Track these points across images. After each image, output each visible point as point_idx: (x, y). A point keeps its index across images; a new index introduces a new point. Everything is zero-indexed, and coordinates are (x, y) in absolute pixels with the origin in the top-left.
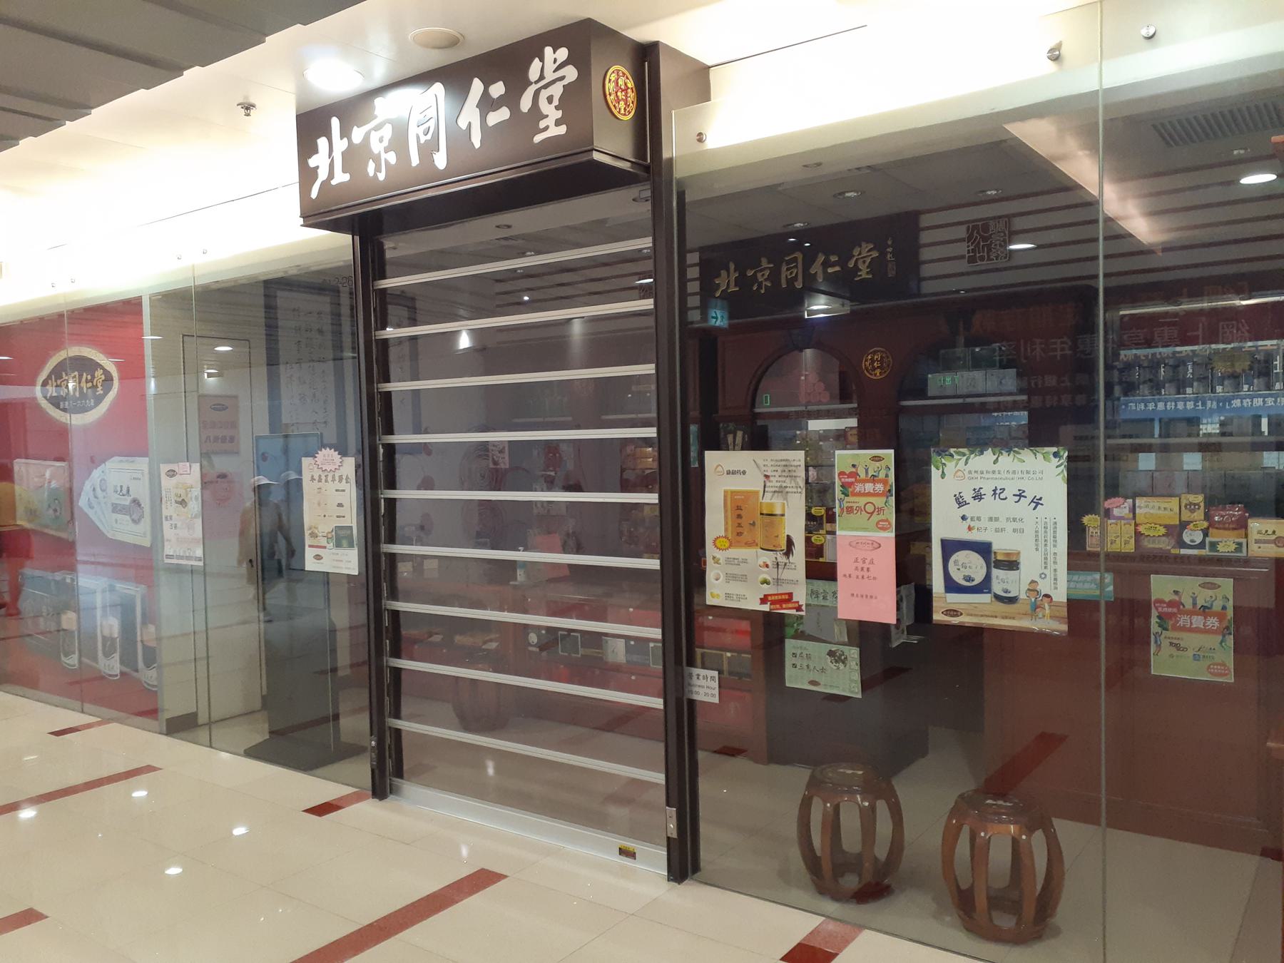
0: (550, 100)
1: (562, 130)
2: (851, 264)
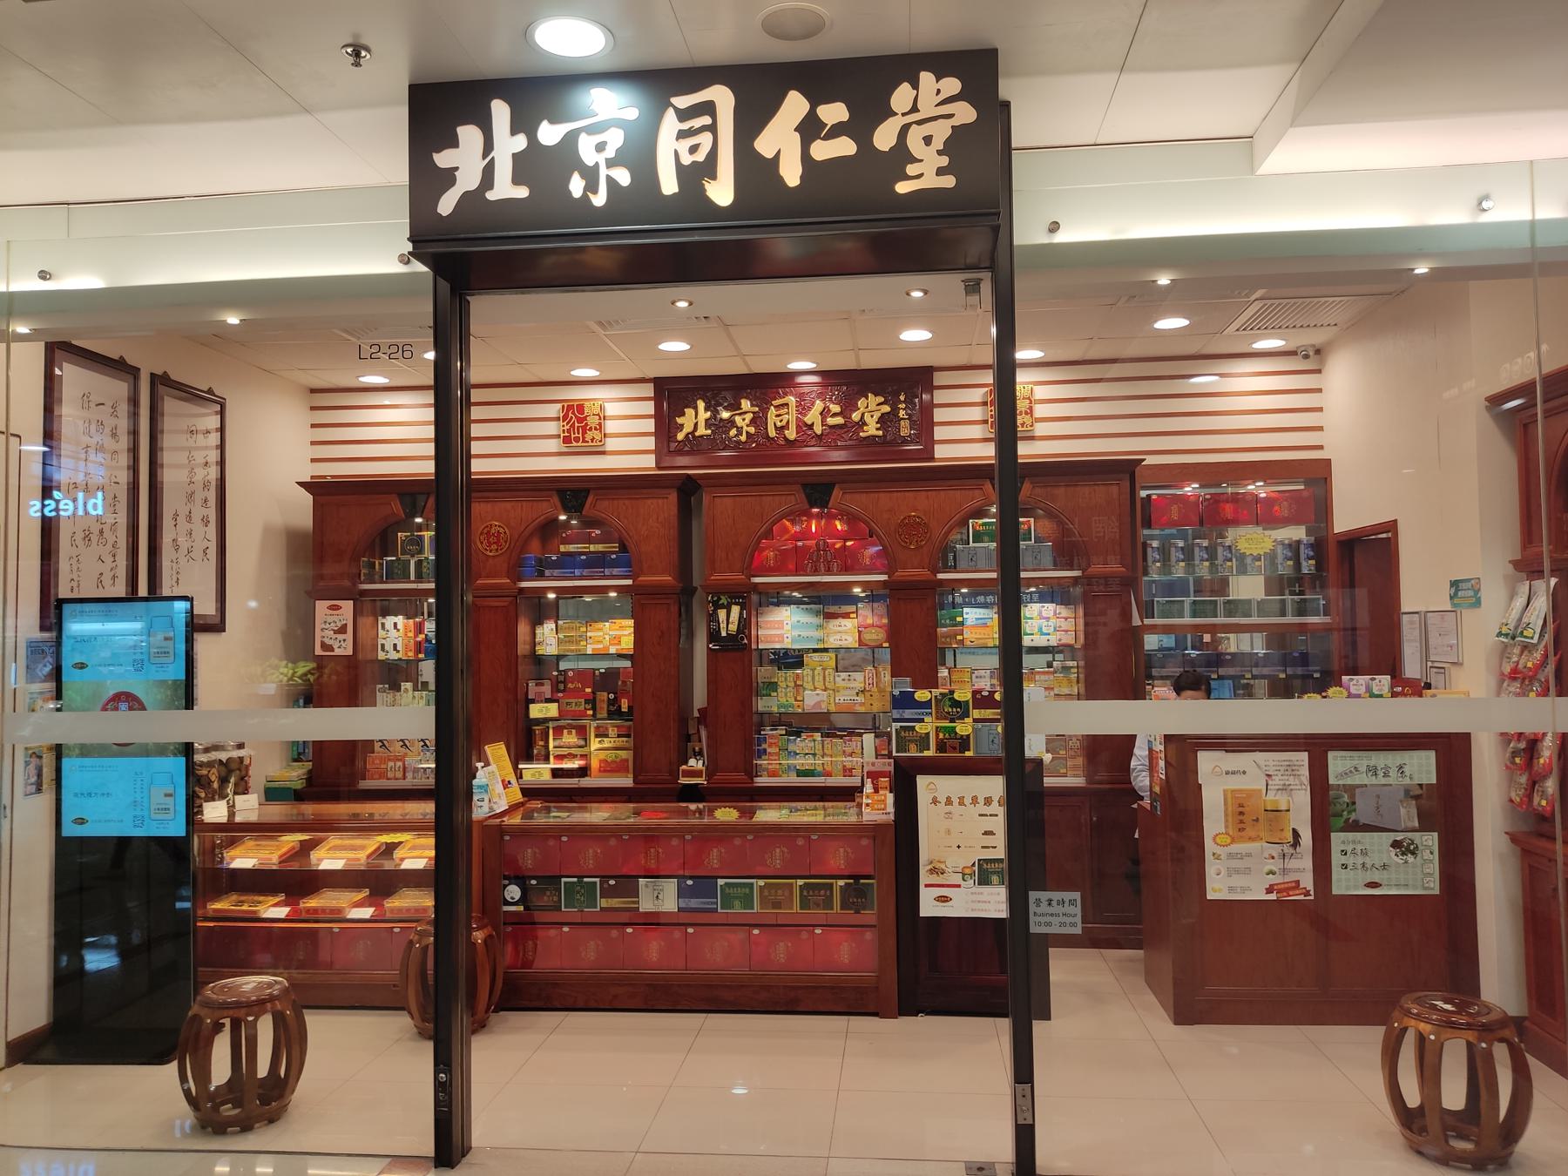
0: (928, 140)
1: (949, 182)
2: (856, 416)
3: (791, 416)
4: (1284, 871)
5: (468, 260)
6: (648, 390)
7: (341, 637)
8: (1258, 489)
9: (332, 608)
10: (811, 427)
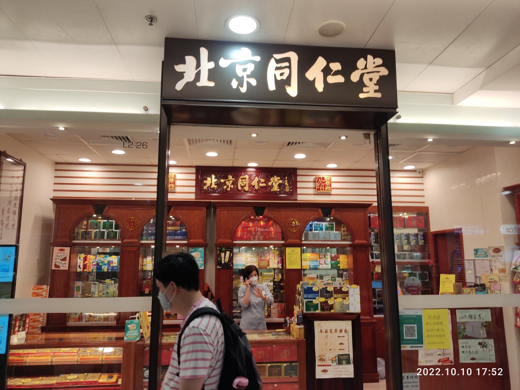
0: (371, 80)
1: (379, 95)
2: (270, 184)
3: (247, 182)
4: (444, 354)
5: (183, 110)
6: (194, 170)
7: (63, 262)
8: (406, 216)
9: (61, 250)
10: (254, 186)
